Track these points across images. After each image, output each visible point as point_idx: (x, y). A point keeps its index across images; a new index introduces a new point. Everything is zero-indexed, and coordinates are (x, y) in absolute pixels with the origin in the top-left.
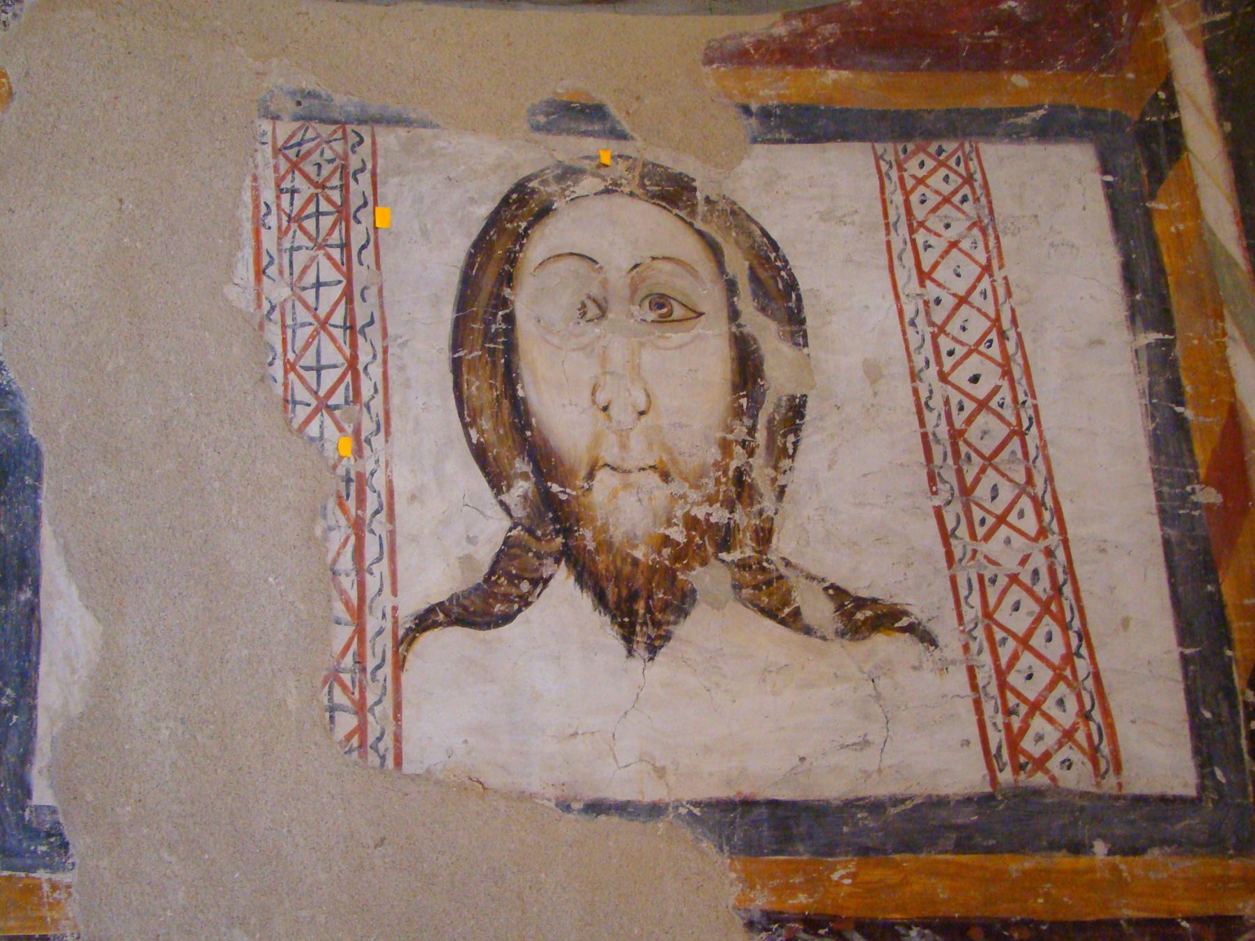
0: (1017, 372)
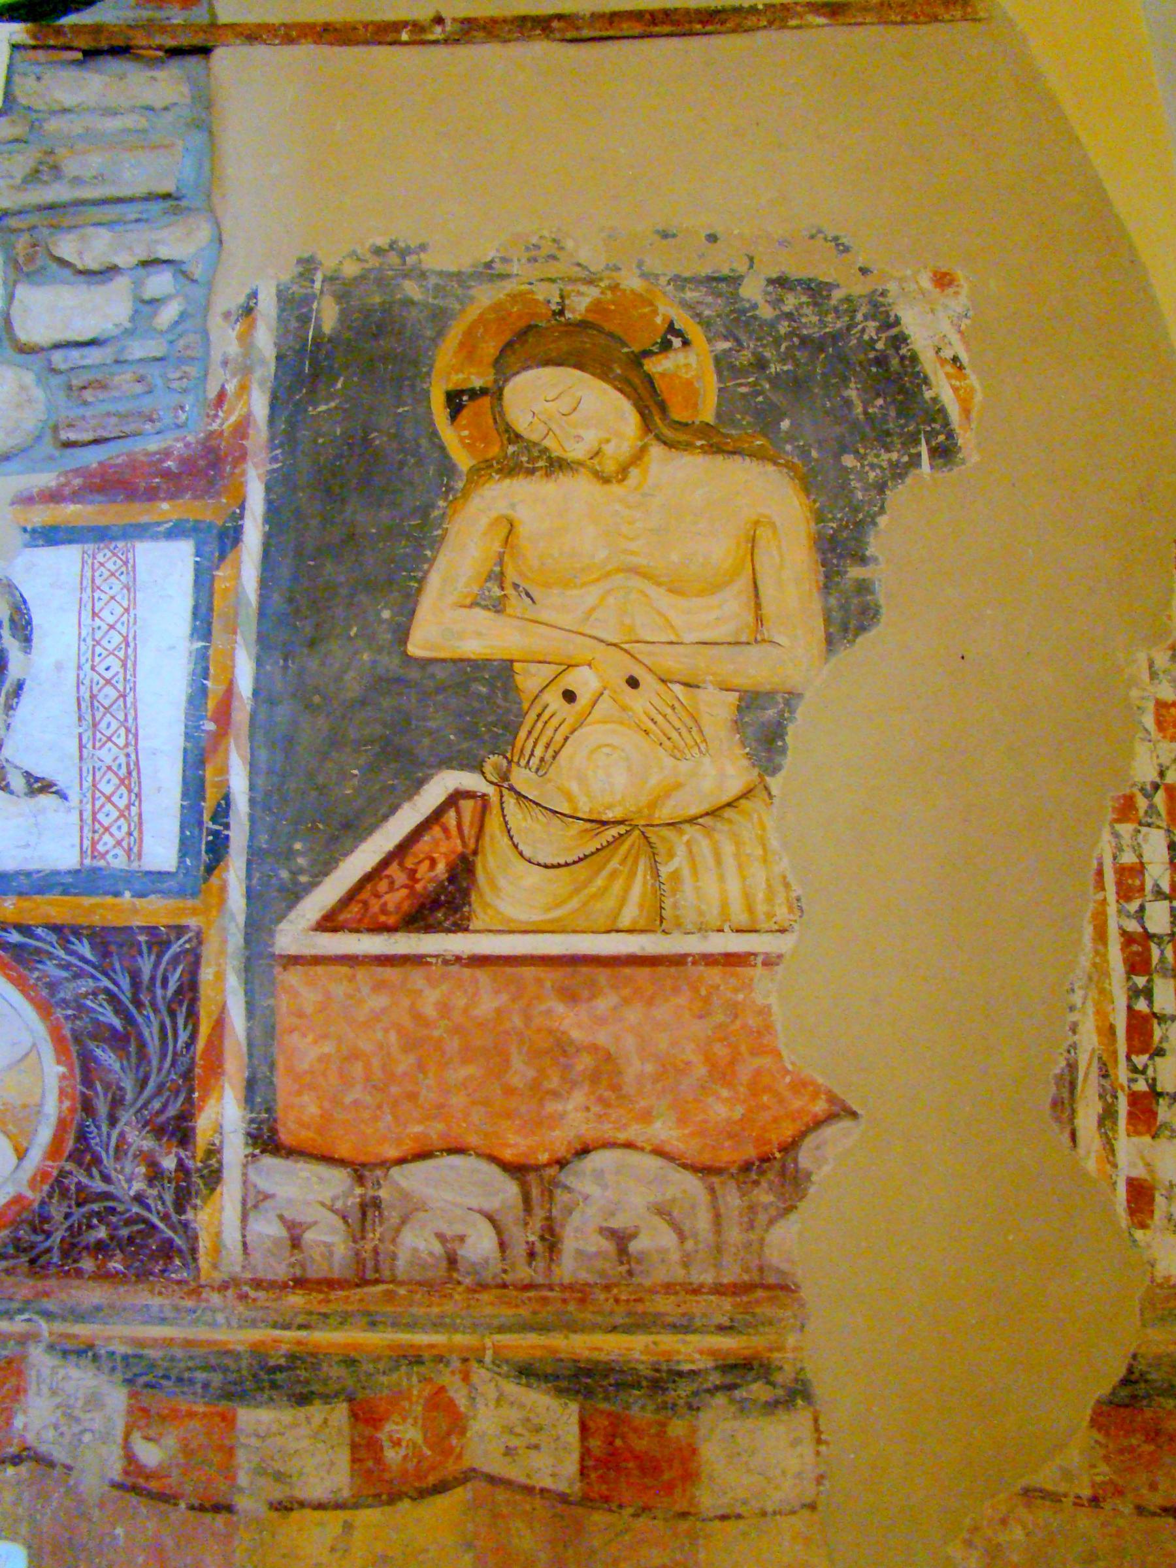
0: (130, 665)
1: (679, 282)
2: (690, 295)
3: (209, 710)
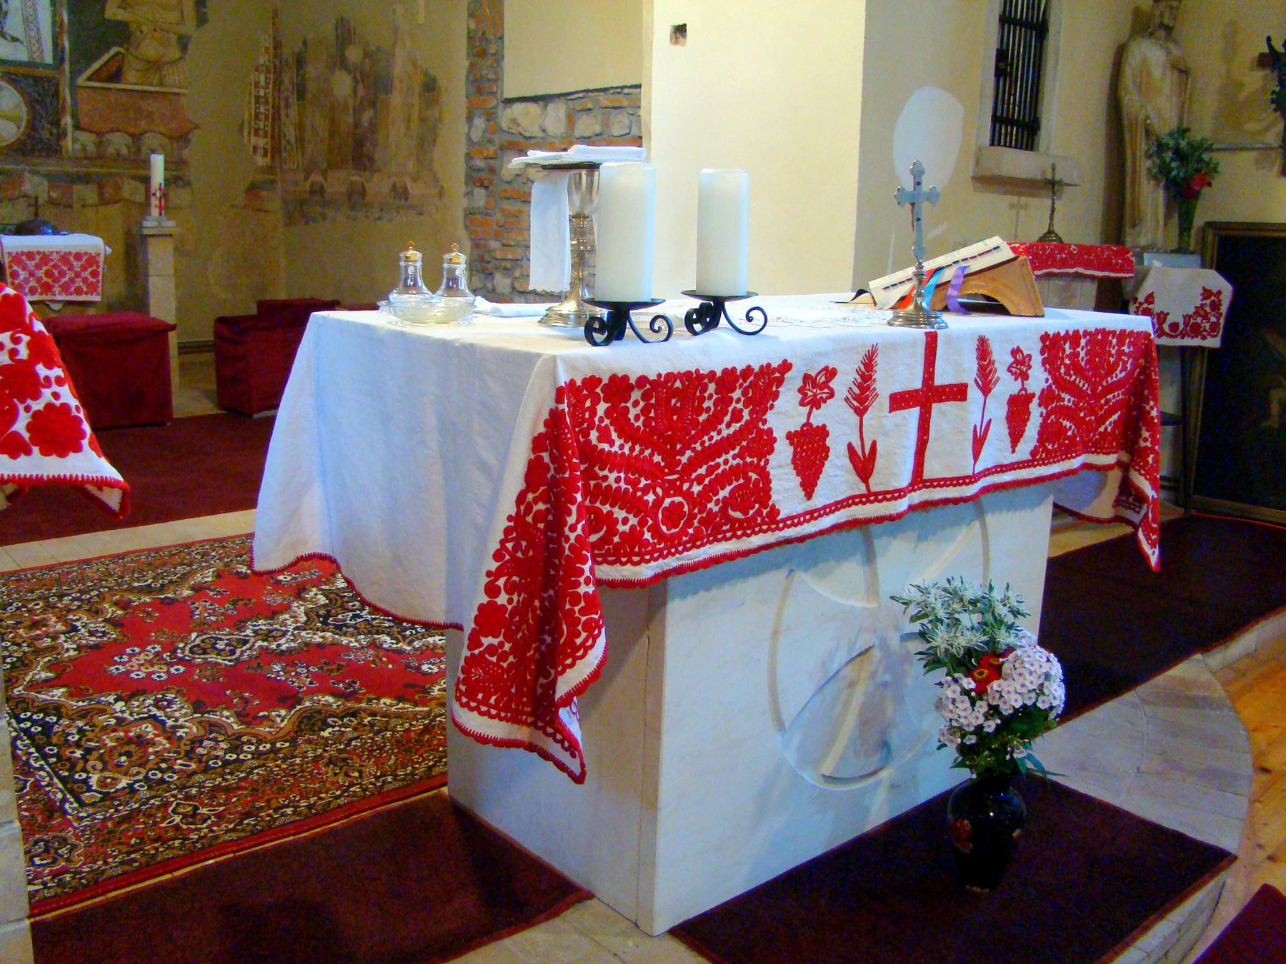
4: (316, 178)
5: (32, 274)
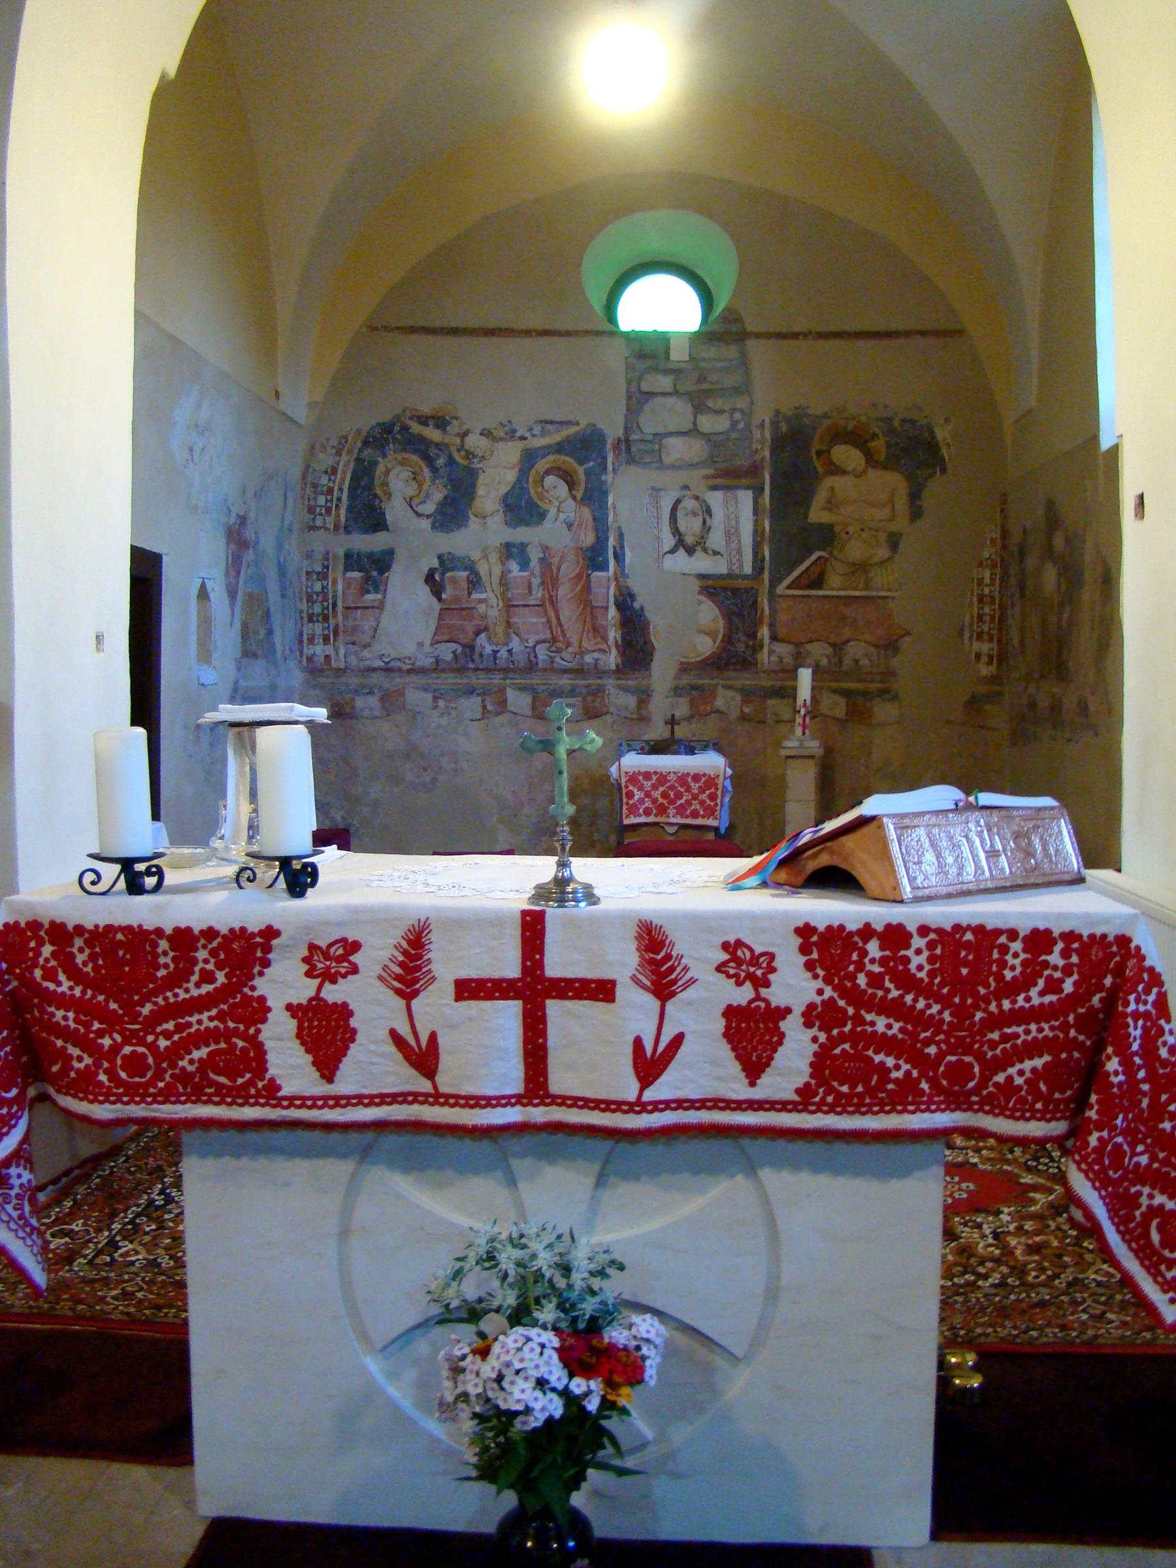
1: (877, 420)
2: (880, 424)
3: (758, 532)
4: (1032, 689)
5: (648, 794)
